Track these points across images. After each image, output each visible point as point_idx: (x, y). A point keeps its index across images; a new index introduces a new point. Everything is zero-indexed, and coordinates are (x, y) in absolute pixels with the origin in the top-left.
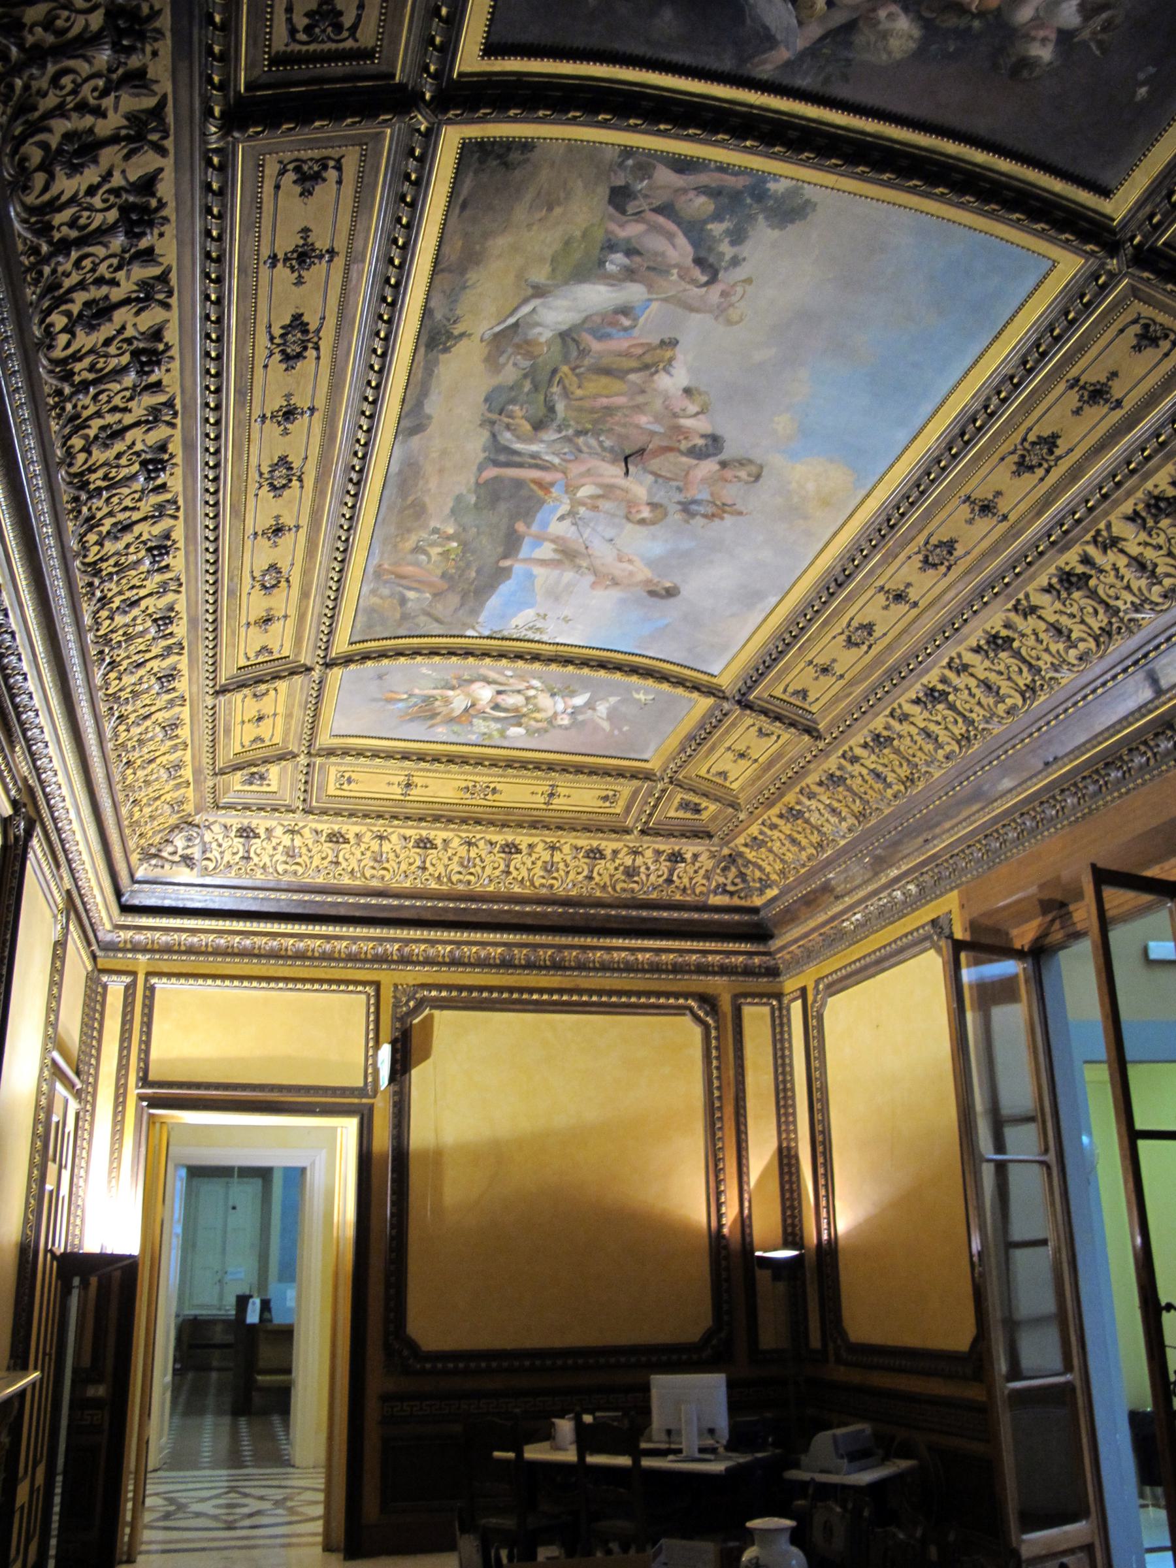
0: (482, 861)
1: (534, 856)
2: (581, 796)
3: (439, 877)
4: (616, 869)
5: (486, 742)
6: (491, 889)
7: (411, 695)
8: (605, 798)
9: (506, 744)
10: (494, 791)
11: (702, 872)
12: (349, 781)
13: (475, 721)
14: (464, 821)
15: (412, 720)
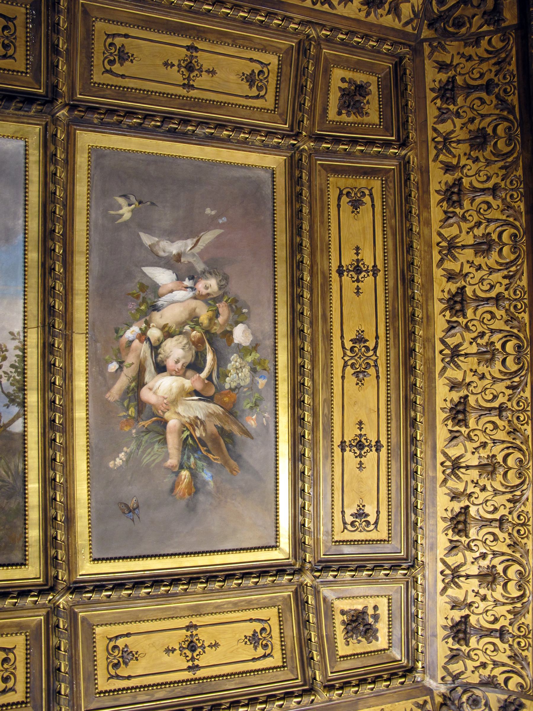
0: (482, 335)
1: (467, 269)
2: (357, 233)
3: (513, 388)
4: (476, 160)
5: (269, 365)
6: (526, 317)
7: (181, 467)
8: (356, 204)
9: (269, 342)
10: (360, 339)
11: (470, 51)
12: (360, 514)
13: (229, 382)
14: (411, 370)
15: (238, 458)
